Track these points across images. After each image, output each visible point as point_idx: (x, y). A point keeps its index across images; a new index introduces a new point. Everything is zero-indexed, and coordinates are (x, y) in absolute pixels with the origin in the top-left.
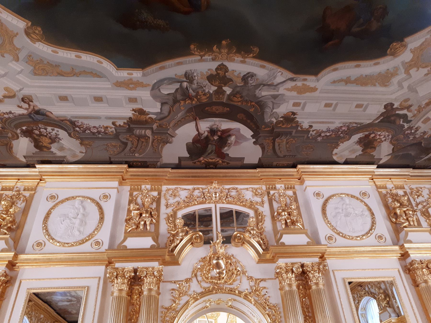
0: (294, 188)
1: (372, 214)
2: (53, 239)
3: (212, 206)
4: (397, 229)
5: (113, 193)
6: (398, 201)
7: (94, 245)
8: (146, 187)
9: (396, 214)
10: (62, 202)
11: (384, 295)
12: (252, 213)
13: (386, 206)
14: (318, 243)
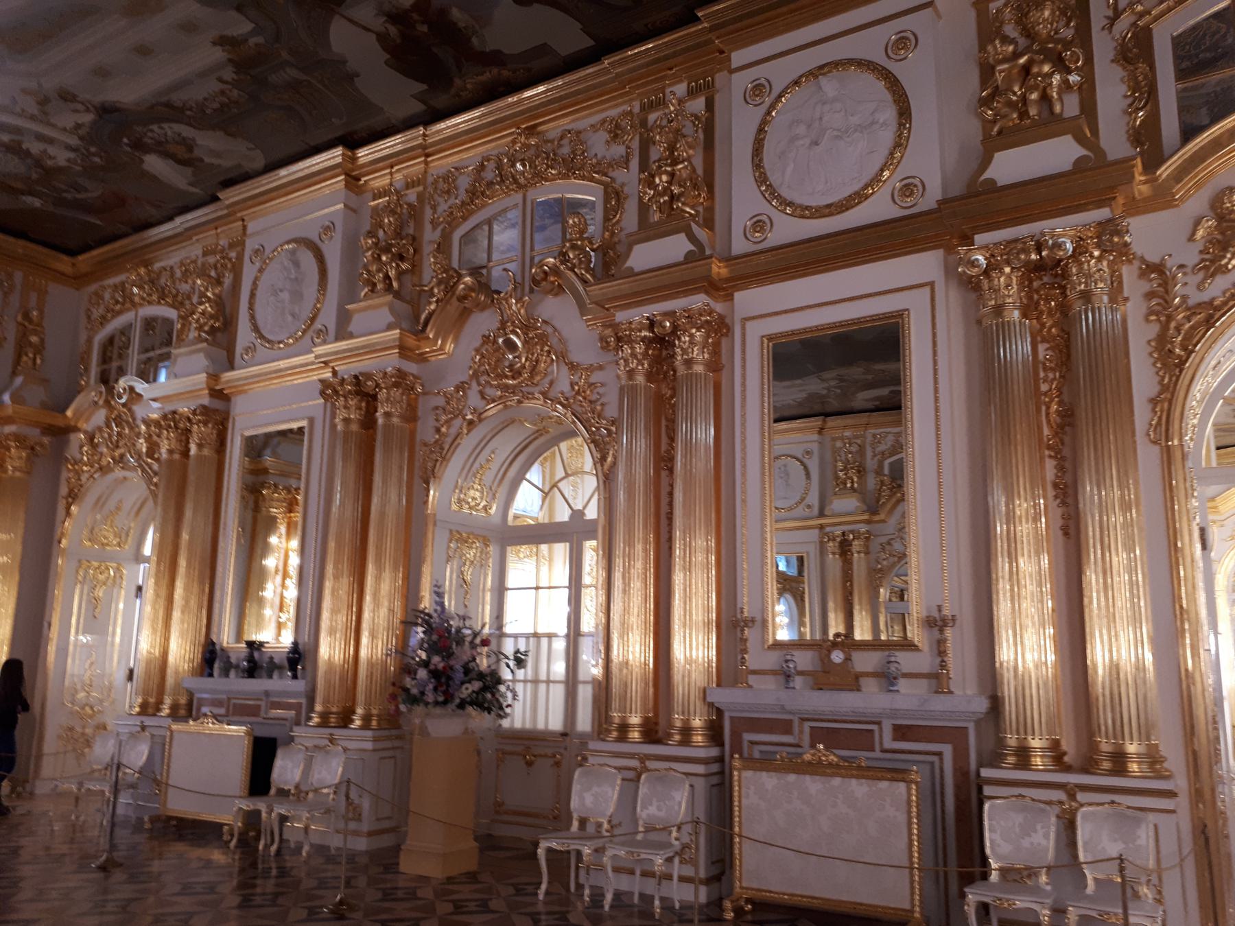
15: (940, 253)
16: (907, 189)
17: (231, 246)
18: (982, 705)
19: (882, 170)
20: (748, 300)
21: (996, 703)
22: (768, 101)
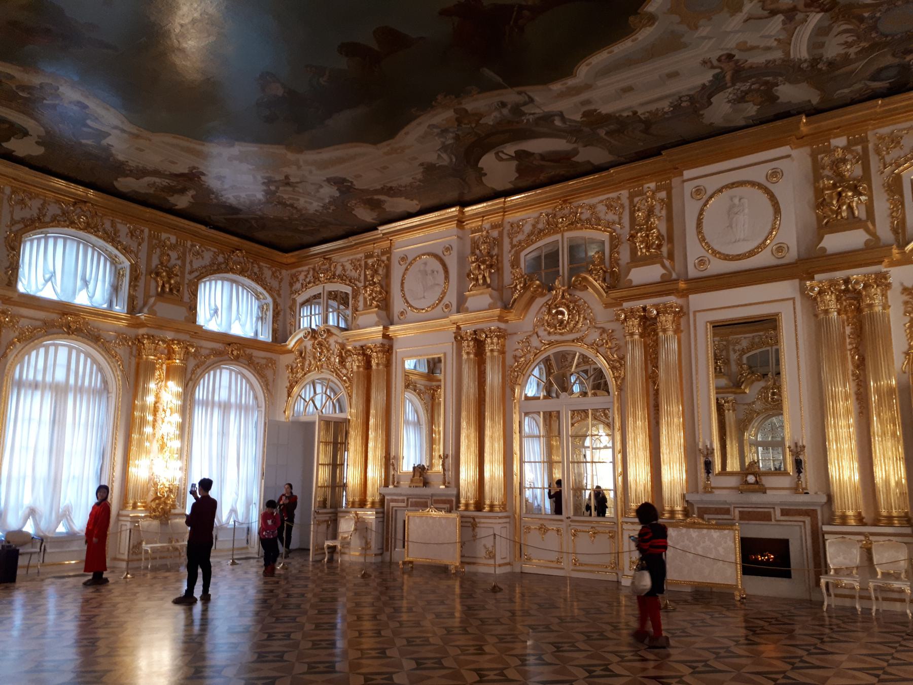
1: (777, 210)
15: (796, 282)
16: (780, 249)
17: (383, 253)
18: (824, 499)
19: (766, 240)
20: (697, 301)
21: (830, 498)
22: (705, 198)
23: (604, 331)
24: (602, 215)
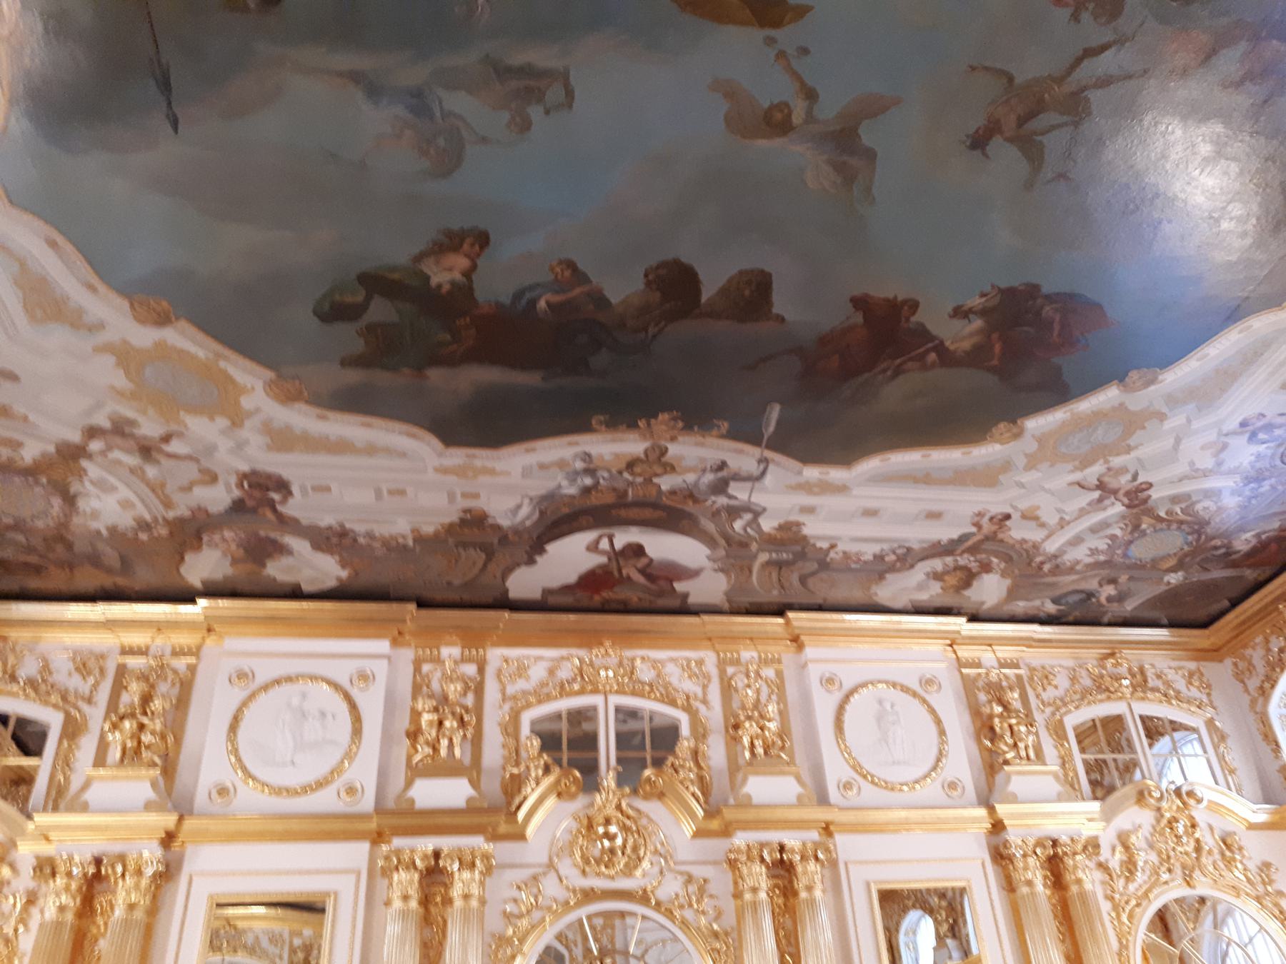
0: (779, 661)
1: (942, 733)
2: (254, 779)
3: (597, 700)
4: (992, 766)
5: (380, 669)
6: (1001, 702)
7: (343, 794)
8: (450, 652)
9: (992, 729)
10: (265, 688)
11: (948, 909)
12: (684, 720)
13: (975, 712)
14: (823, 800)
23: (690, 879)
24: (674, 681)
